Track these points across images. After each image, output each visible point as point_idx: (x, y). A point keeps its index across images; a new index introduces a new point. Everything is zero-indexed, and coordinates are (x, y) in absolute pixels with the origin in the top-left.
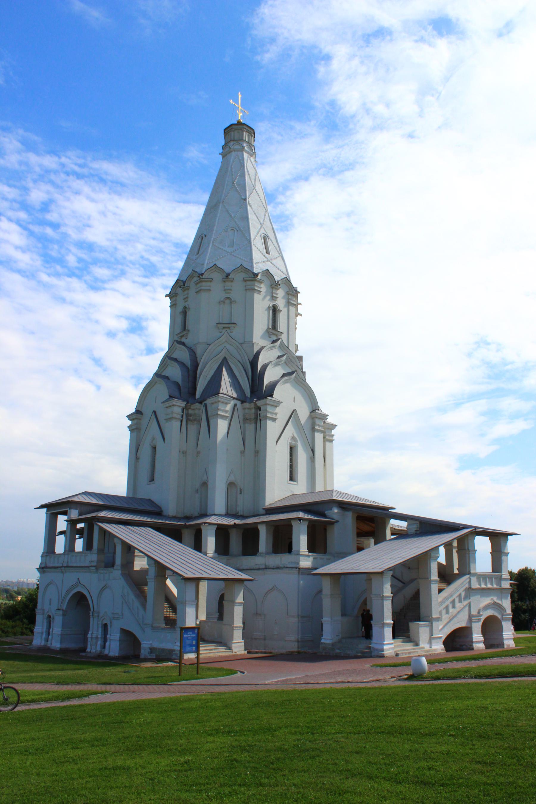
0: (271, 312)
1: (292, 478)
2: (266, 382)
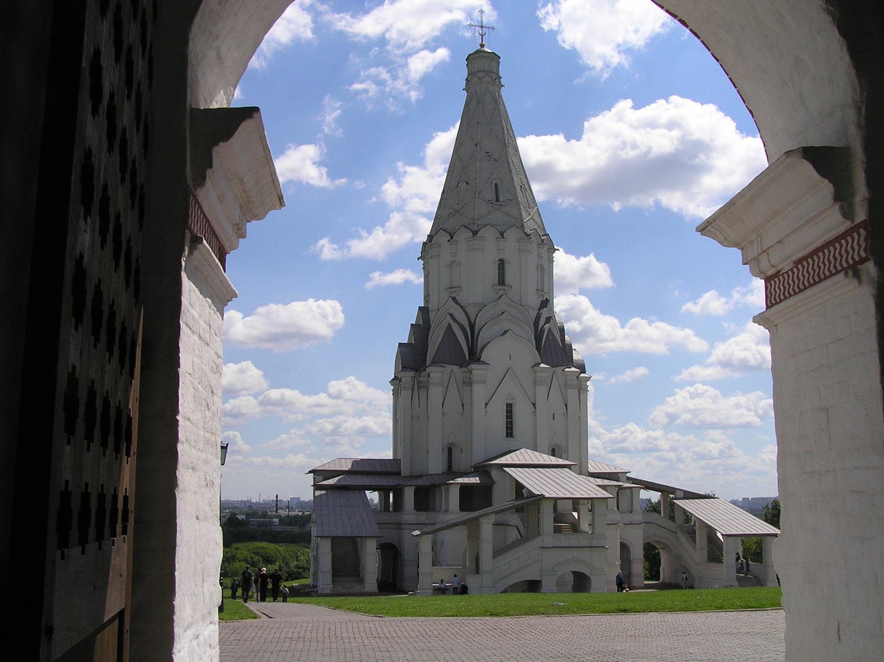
0: (497, 267)
1: (510, 433)
2: (480, 343)
